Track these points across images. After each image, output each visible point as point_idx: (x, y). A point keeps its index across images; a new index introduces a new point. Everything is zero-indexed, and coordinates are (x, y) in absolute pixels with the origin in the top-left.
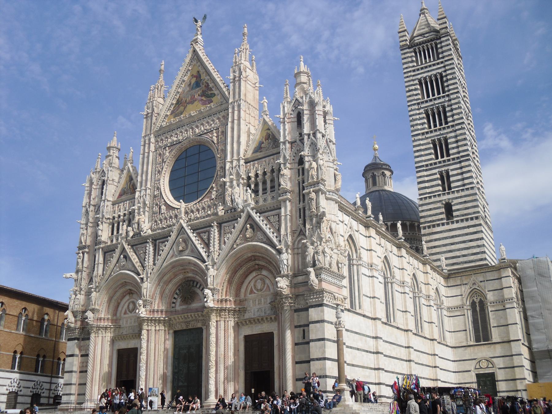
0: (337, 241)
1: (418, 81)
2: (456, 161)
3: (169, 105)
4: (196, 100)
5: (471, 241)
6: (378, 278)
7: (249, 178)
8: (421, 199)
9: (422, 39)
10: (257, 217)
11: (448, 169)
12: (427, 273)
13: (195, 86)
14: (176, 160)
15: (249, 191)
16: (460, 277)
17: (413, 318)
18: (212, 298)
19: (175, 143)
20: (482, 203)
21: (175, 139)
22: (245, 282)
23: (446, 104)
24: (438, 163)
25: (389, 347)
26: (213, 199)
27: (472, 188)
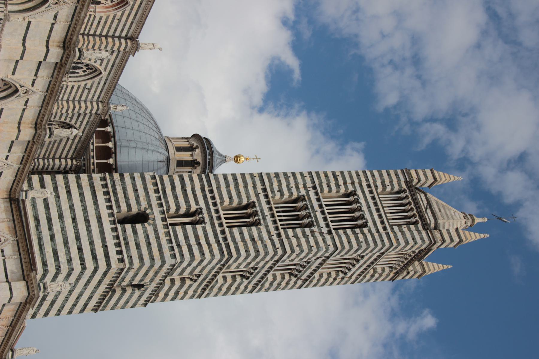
2: (220, 236)
5: (80, 249)
8: (154, 178)
9: (423, 203)
11: (205, 223)
16: (11, 218)
20: (147, 280)
23: (315, 229)
27: (174, 256)
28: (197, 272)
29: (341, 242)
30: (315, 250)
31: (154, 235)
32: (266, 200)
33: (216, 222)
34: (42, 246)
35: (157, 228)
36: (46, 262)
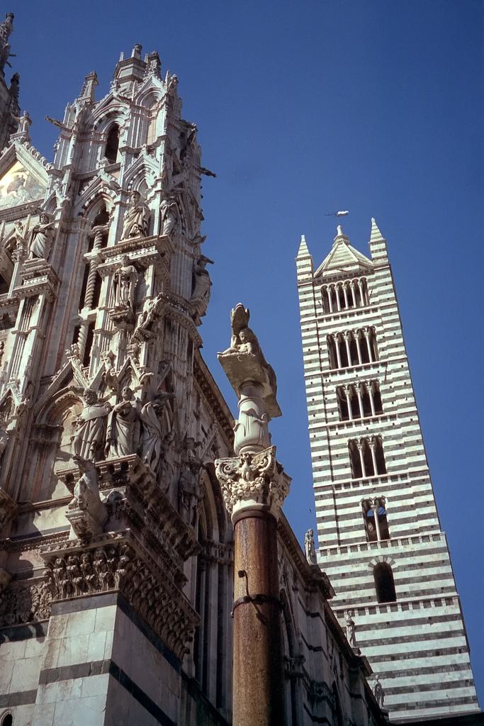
1: (327, 339)
2: (400, 482)
5: (438, 653)
11: (383, 498)
29: (397, 354)
31: (408, 559)
32: (345, 427)
33: (380, 485)
34: (438, 702)
35: (397, 554)
36: (462, 698)
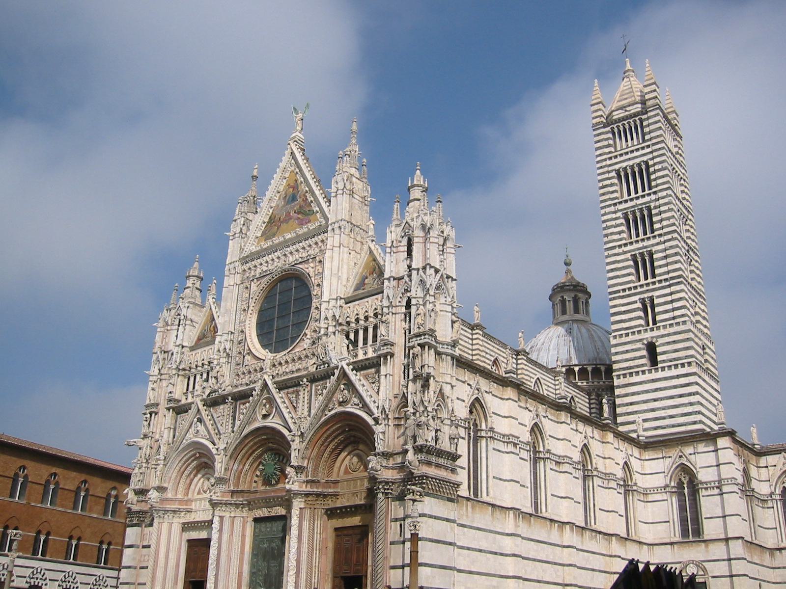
0: (451, 409)
1: (616, 173)
2: (664, 284)
3: (260, 224)
4: (291, 219)
5: (681, 396)
6: (518, 455)
7: (348, 323)
8: (615, 337)
10: (352, 375)
11: (653, 296)
12: (608, 442)
13: (291, 199)
14: (266, 298)
15: (347, 342)
17: (582, 506)
18: (296, 478)
19: (265, 274)
20: (700, 343)
21: (265, 269)
22: (339, 457)
24: (639, 288)
25: (535, 547)
26: (305, 349)
27: (684, 322)
28: (691, 302)
30: (672, 206)
33: (651, 287)
